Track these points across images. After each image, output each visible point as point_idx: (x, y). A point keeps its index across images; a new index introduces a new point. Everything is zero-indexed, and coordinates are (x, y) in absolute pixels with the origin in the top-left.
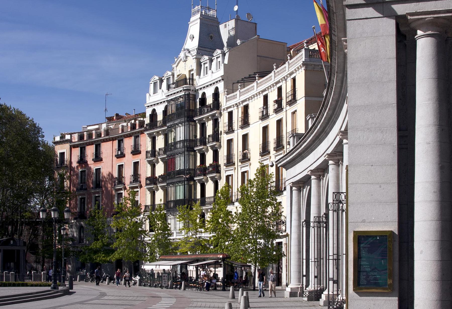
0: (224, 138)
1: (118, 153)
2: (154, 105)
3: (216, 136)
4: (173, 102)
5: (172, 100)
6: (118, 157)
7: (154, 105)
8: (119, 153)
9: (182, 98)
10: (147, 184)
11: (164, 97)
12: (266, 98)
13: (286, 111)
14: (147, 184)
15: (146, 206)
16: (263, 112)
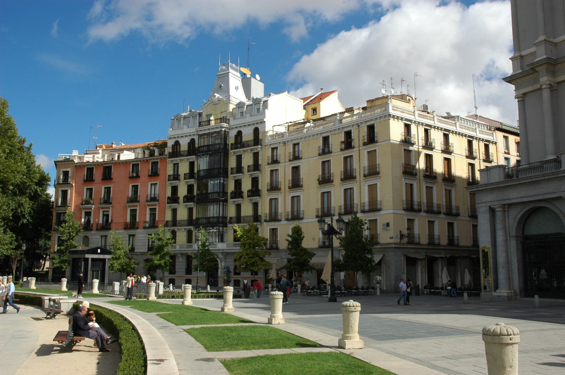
0: (266, 170)
1: (133, 175)
2: (178, 137)
3: (256, 166)
4: (205, 136)
5: (204, 134)
6: (131, 178)
7: (178, 137)
8: (135, 175)
9: (218, 133)
10: (184, 202)
11: (195, 131)
12: (326, 140)
13: (359, 150)
14: (168, 203)
15: (167, 222)
16: (323, 150)
